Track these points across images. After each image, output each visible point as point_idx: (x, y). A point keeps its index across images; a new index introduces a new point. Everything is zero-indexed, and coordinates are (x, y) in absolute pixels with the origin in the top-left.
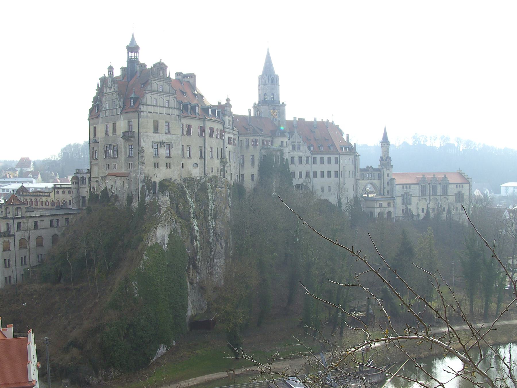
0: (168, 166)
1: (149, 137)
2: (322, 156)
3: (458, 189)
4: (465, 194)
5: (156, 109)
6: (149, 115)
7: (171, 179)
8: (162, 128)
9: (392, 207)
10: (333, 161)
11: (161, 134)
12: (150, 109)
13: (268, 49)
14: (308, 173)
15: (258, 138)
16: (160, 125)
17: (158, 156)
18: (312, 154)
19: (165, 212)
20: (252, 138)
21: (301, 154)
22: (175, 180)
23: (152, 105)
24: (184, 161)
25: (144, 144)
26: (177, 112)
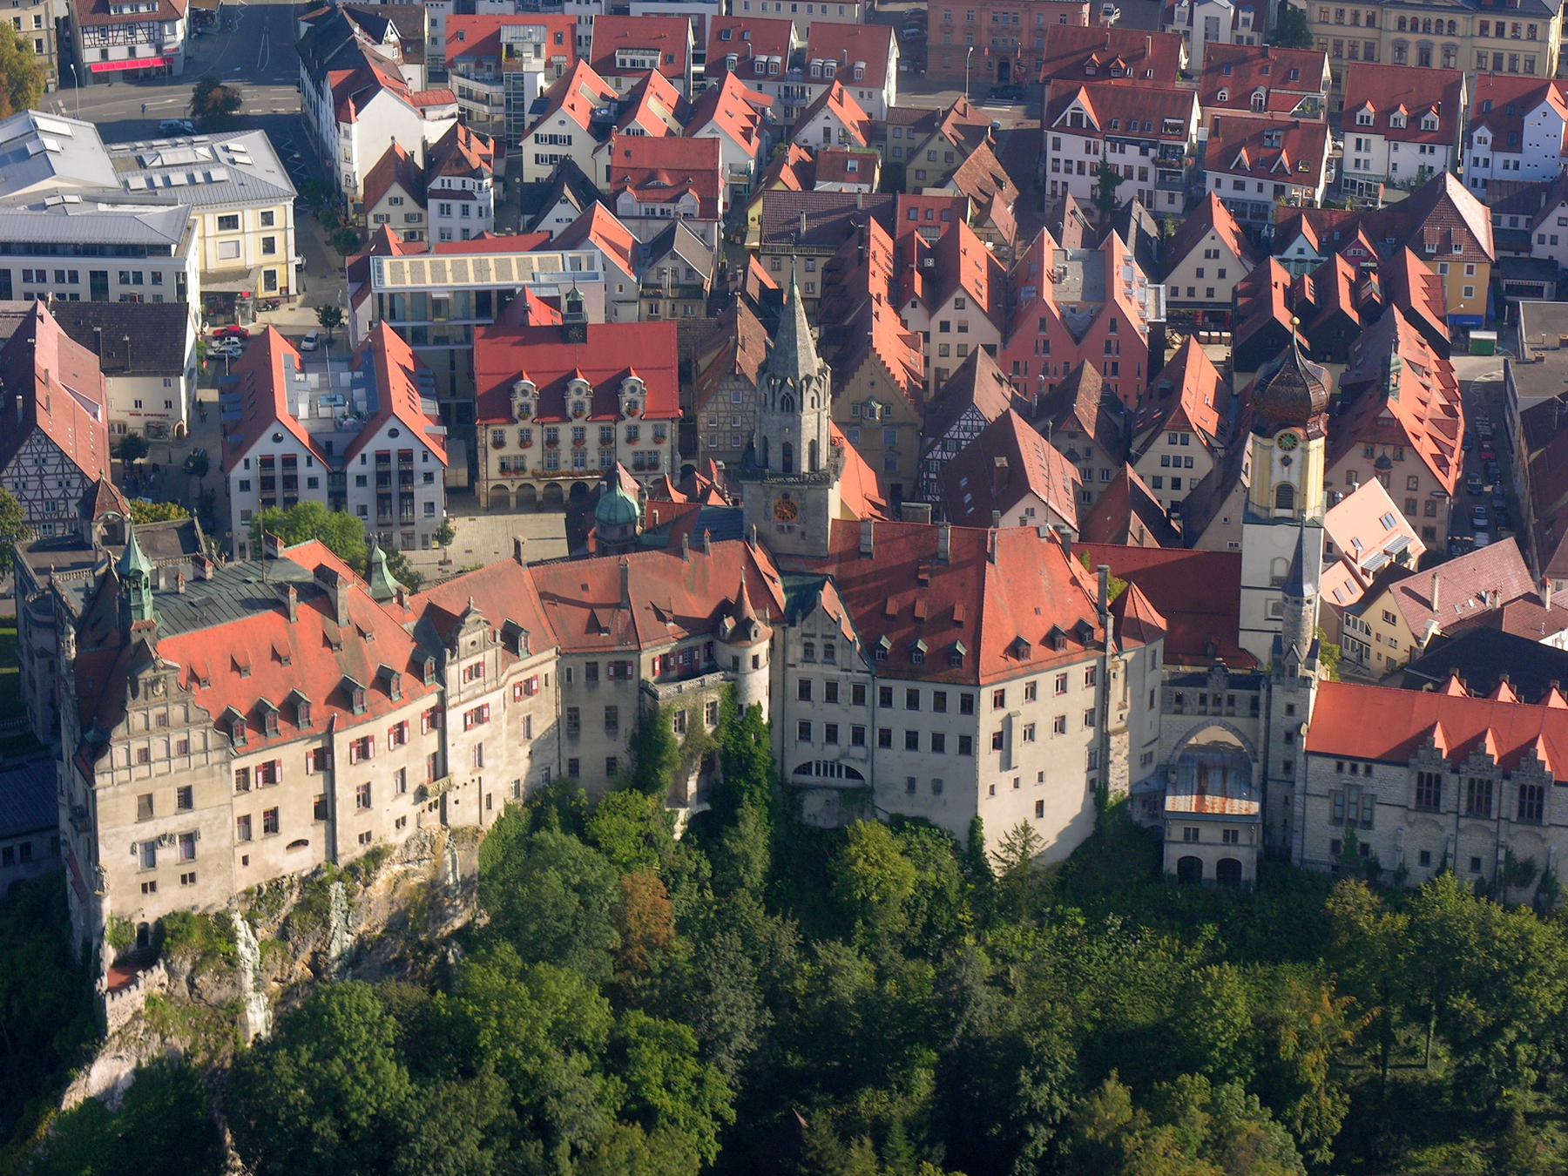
1: (123, 836)
6: (122, 789)
9: (1244, 846)
10: (954, 702)
11: (162, 818)
17: (151, 862)
19: (113, 1035)
21: (834, 672)
24: (247, 849)
25: (107, 853)
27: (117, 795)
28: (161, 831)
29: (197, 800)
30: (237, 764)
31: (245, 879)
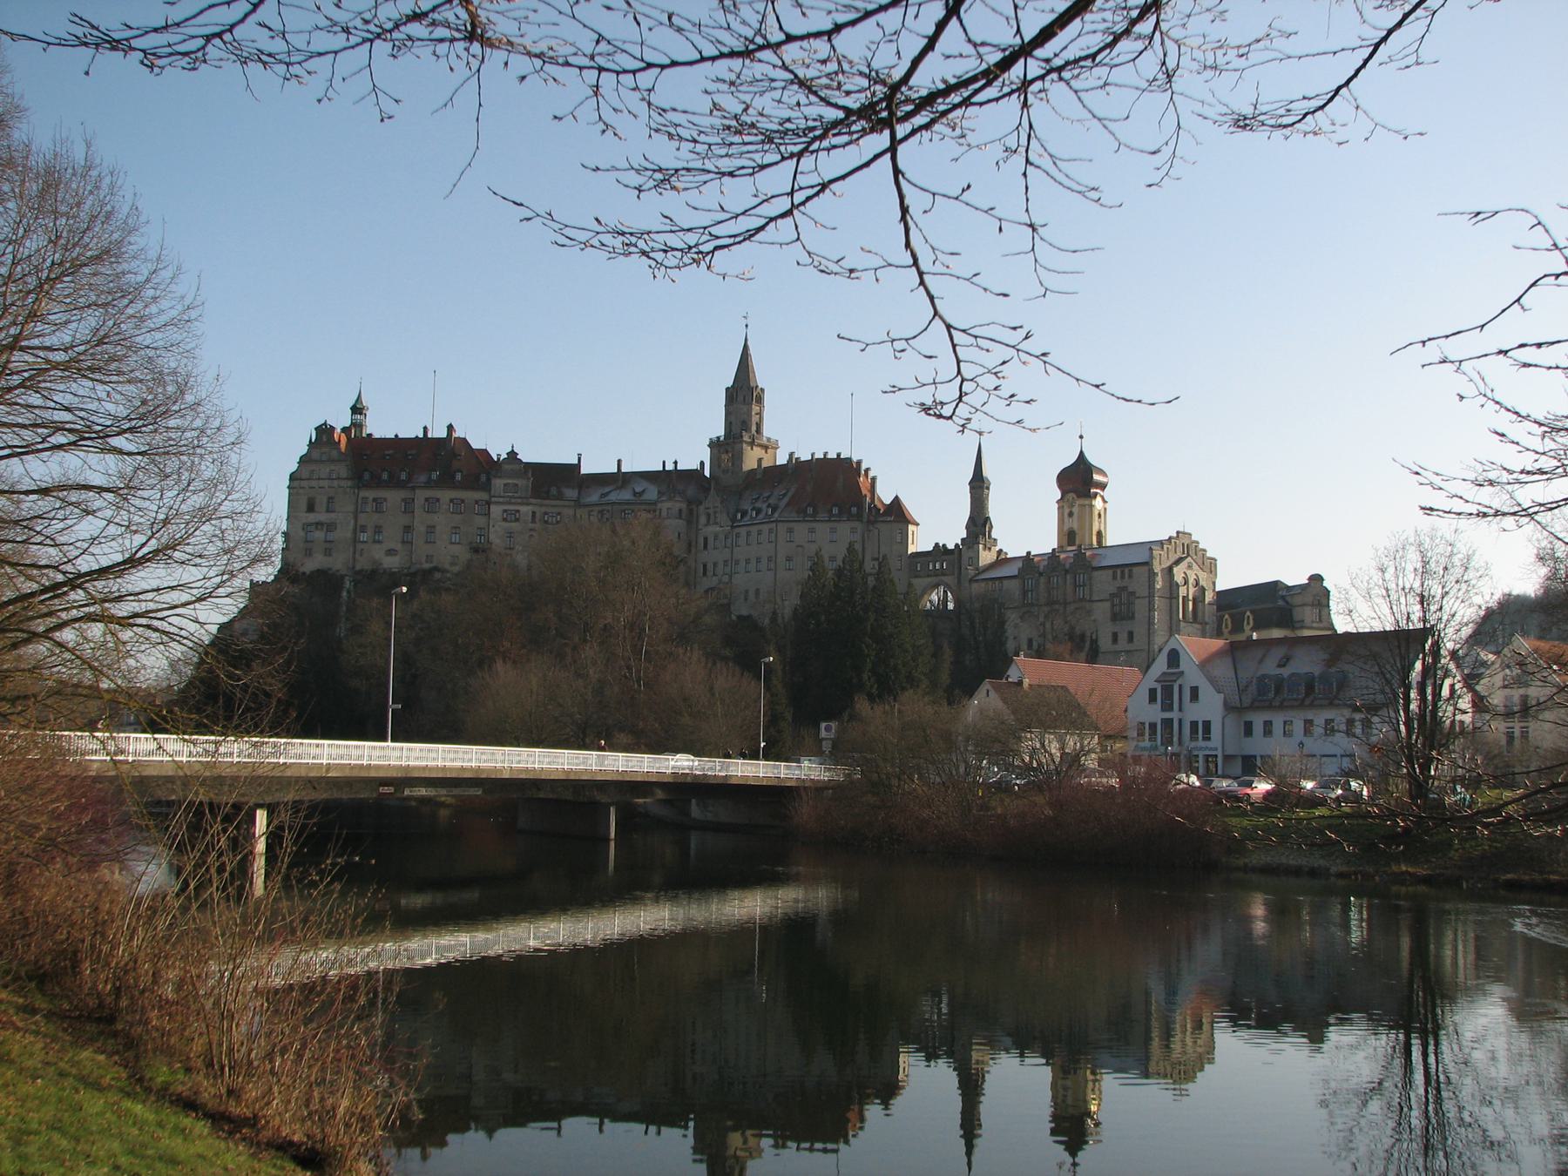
0: (328, 553)
3: (1119, 583)
4: (1137, 595)
5: (314, 483)
6: (301, 491)
7: (330, 569)
8: (321, 501)
12: (304, 483)
13: (746, 340)
15: (609, 508)
20: (600, 509)
26: (349, 483)
28: (317, 520)
30: (364, 493)
31: (363, 564)
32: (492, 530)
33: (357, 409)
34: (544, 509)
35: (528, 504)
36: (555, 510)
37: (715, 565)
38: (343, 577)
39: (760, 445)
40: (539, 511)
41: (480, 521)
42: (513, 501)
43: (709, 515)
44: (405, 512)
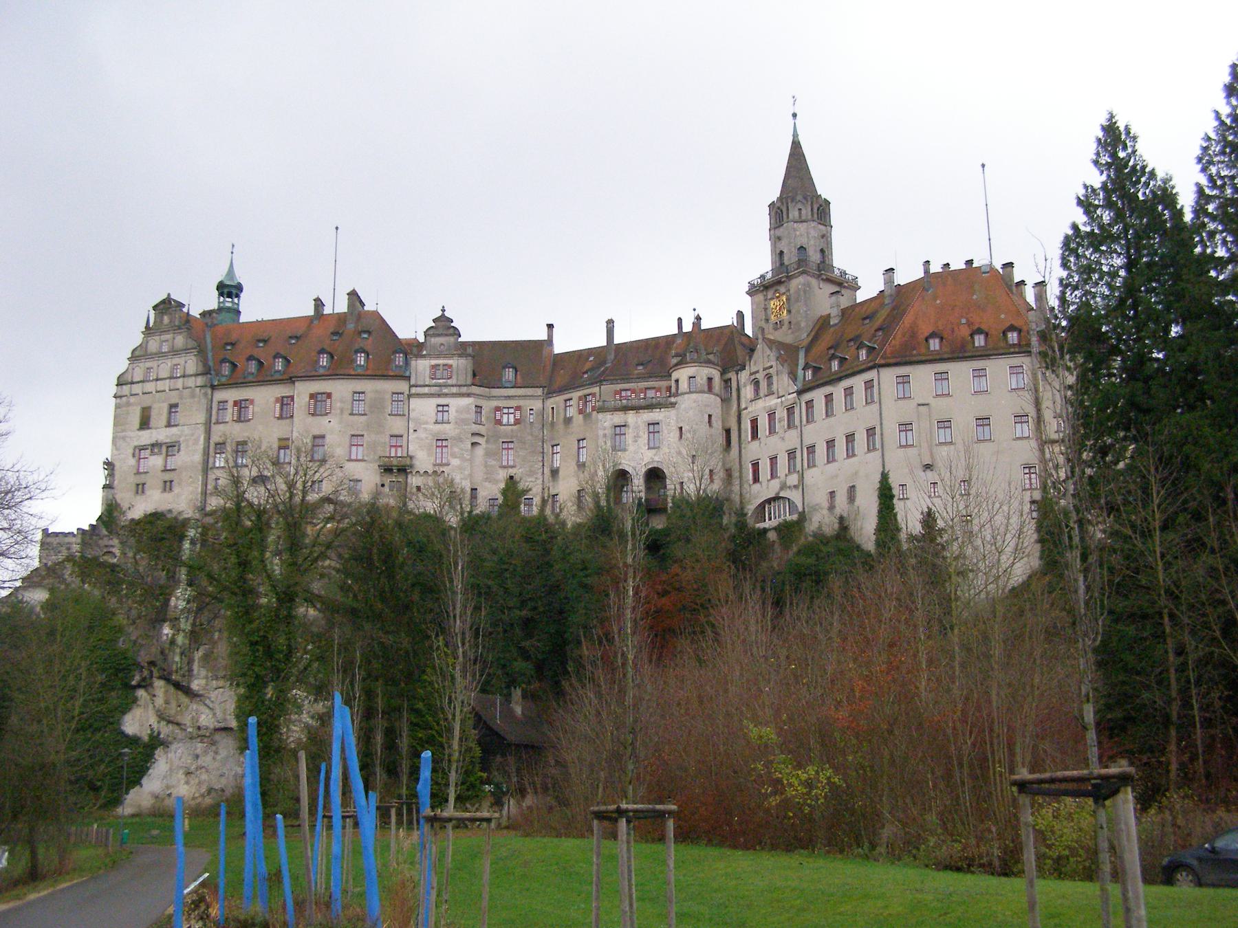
0: (168, 486)
1: (128, 440)
2: (827, 389)
5: (150, 387)
6: (132, 400)
7: (170, 511)
8: (159, 415)
11: (156, 428)
12: (137, 389)
13: (795, 135)
14: (791, 454)
15: (596, 390)
16: (154, 414)
18: (800, 393)
22: (180, 513)
23: (138, 382)
26: (200, 381)
27: (128, 404)
28: (153, 441)
29: (179, 417)
30: (220, 395)
32: (412, 436)
33: (229, 290)
34: (495, 403)
35: (469, 395)
36: (513, 403)
37: (773, 460)
38: (185, 523)
39: (830, 281)
40: (488, 405)
41: (397, 425)
42: (445, 391)
43: (756, 383)
44: (278, 418)
